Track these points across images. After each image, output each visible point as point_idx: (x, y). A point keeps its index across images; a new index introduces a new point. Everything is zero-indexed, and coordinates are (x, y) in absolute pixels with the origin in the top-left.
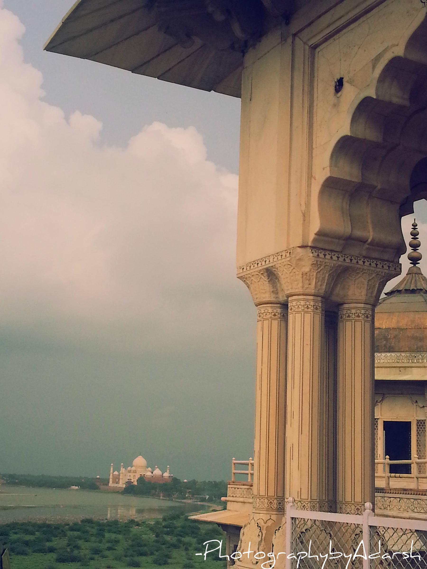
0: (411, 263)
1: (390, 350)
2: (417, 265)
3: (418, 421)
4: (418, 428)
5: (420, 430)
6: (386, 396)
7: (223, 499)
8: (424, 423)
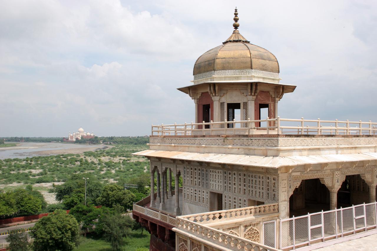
0: (234, 28)
2: (237, 29)
3: (244, 103)
4: (244, 106)
5: (244, 107)
8: (247, 103)
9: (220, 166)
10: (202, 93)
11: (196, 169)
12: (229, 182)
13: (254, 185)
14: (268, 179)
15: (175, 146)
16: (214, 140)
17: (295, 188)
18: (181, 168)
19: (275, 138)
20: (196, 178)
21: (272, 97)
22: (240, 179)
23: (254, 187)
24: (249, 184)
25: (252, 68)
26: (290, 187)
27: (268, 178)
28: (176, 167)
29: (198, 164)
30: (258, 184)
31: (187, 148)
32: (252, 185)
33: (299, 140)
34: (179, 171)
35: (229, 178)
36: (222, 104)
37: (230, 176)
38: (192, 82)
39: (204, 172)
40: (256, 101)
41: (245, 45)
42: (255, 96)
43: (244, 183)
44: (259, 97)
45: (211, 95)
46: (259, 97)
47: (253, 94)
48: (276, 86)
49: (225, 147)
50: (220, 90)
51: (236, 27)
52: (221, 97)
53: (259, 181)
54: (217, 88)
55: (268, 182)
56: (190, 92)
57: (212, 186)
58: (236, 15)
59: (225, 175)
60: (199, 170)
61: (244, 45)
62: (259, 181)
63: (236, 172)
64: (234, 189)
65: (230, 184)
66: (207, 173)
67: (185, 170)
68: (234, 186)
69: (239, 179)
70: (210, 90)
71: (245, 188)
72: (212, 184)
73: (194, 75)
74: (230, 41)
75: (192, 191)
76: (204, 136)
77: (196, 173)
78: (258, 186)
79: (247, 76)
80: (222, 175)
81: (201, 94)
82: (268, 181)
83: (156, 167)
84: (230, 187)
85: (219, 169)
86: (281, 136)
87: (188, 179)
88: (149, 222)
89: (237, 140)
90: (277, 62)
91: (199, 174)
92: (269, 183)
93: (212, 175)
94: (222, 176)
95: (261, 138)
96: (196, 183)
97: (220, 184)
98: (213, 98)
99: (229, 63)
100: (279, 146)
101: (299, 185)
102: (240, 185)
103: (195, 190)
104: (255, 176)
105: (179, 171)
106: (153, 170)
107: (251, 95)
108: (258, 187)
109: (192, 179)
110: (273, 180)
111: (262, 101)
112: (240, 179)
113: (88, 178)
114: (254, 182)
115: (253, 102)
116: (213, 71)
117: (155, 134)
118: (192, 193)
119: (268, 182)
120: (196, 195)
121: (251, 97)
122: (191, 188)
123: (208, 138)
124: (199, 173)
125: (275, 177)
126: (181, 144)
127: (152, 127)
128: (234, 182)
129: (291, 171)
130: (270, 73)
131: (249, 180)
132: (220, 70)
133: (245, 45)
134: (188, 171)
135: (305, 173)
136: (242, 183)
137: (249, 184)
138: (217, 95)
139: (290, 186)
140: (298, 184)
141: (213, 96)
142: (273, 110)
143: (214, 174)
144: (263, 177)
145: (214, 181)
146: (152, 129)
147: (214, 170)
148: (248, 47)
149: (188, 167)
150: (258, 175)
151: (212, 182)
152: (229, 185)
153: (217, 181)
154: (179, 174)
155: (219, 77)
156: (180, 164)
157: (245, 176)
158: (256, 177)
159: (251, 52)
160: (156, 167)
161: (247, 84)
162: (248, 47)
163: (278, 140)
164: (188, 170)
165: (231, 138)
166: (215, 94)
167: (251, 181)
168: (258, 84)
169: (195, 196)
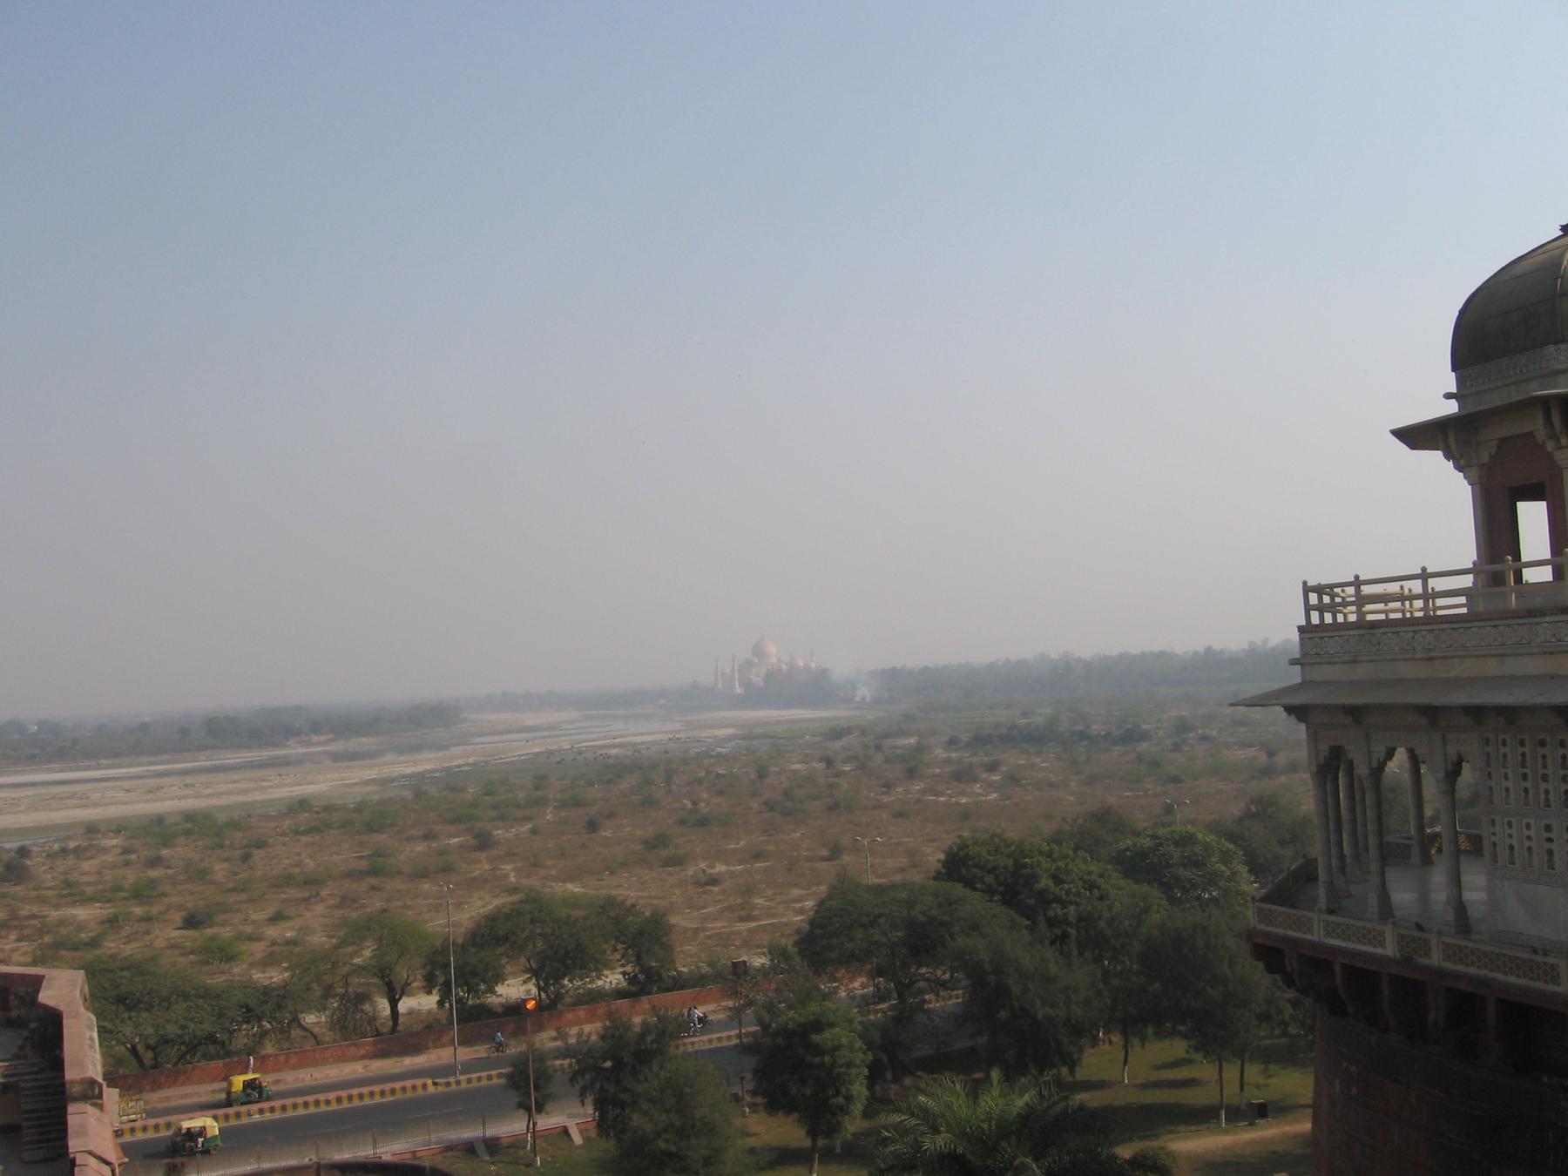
10: (1502, 441)
11: (1543, 744)
20: (1545, 778)
28: (1444, 741)
38: (1448, 396)
45: (1550, 446)
56: (1446, 439)
75: (1532, 833)
77: (1549, 760)
81: (1499, 446)
83: (1336, 754)
88: (1337, 968)
96: (1547, 800)
103: (1548, 828)
106: (1322, 761)
116: (1552, 348)
118: (1529, 838)
120: (1554, 846)
127: (1307, 589)
134: (1505, 756)
141: (1561, 448)
164: (1503, 750)
169: (1550, 853)
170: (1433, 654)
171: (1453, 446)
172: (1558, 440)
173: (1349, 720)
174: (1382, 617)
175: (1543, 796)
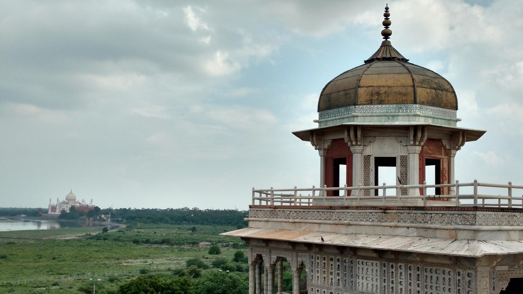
1: (381, 102)
3: (402, 157)
6: (377, 138)
7: (245, 219)
9: (375, 255)
10: (334, 141)
11: (332, 260)
12: (391, 279)
13: (434, 285)
14: (459, 275)
15: (295, 223)
16: (365, 214)
17: (500, 290)
18: (305, 258)
19: (471, 213)
21: (445, 149)
22: (410, 274)
23: (434, 288)
24: (425, 284)
25: (415, 102)
26: (494, 289)
27: (459, 273)
28: (297, 256)
29: (336, 251)
30: (442, 283)
31: (317, 226)
32: (431, 284)
33: (506, 216)
34: (302, 262)
35: (391, 274)
36: (367, 159)
37: (394, 270)
38: (315, 121)
39: (347, 265)
40: (421, 155)
41: (404, 65)
42: (421, 147)
43: (418, 282)
44: (425, 147)
45: (349, 144)
46: (425, 147)
47: (417, 143)
48: (452, 132)
49: (384, 224)
50: (364, 136)
51: (386, 35)
52: (365, 147)
53: (444, 279)
54: (359, 133)
55: (459, 280)
56: (312, 137)
57: (361, 286)
58: (387, 15)
59: (384, 269)
60: (338, 260)
61: (400, 65)
62: (444, 279)
63: (403, 265)
64: (399, 291)
65: (392, 282)
66: (352, 265)
67: (313, 260)
68: (400, 287)
69: (409, 276)
70: (349, 135)
71: (418, 289)
72: (360, 284)
73: (318, 111)
74: (378, 59)
76: (347, 208)
77: (333, 266)
78: (442, 286)
79: (408, 115)
80: (378, 268)
82: (458, 278)
84: (392, 288)
85: (374, 260)
86: (480, 209)
87: (319, 275)
89: (405, 214)
90: (454, 92)
91: (339, 268)
92: (461, 281)
93: (361, 270)
94: (378, 271)
95: (446, 212)
96: (332, 282)
97: (375, 283)
98: (352, 149)
99: (378, 94)
100: (477, 224)
101: (506, 287)
102: (410, 283)
104: (436, 270)
105: (302, 262)
106: (253, 260)
107: (415, 145)
108: (442, 288)
109: (325, 275)
110: (467, 276)
111: (431, 154)
112: (410, 274)
113: (100, 280)
114: (434, 279)
115: (417, 157)
117: (257, 203)
119: (459, 280)
121: (413, 148)
122: (323, 290)
123: (354, 211)
124: (339, 265)
125: (470, 271)
126: (307, 219)
127: (254, 192)
128: (399, 280)
129: (494, 264)
130: (443, 109)
131: (426, 276)
132: (364, 104)
133: (404, 65)
135: (516, 267)
136: (414, 282)
137: (425, 284)
138: (359, 143)
139: (494, 287)
140: (504, 285)
141: (352, 145)
142: (447, 169)
143: (365, 267)
144: (449, 271)
145: (364, 278)
146: (253, 195)
147: (365, 261)
148: (408, 70)
149: (317, 256)
150: (442, 269)
151: (360, 281)
152: (391, 285)
153: (370, 279)
154: (301, 268)
155: (364, 116)
156: (304, 252)
157: (418, 270)
158: (438, 271)
159: (415, 76)
160: (260, 258)
161: (407, 128)
162: (408, 70)
163: (475, 215)
164: (317, 261)
165: (395, 211)
166: (357, 142)
167: (429, 279)
168: (426, 129)
170: (296, 220)
171: (315, 141)
172: (352, 142)
173: (264, 245)
174: (288, 204)
175: (330, 281)
